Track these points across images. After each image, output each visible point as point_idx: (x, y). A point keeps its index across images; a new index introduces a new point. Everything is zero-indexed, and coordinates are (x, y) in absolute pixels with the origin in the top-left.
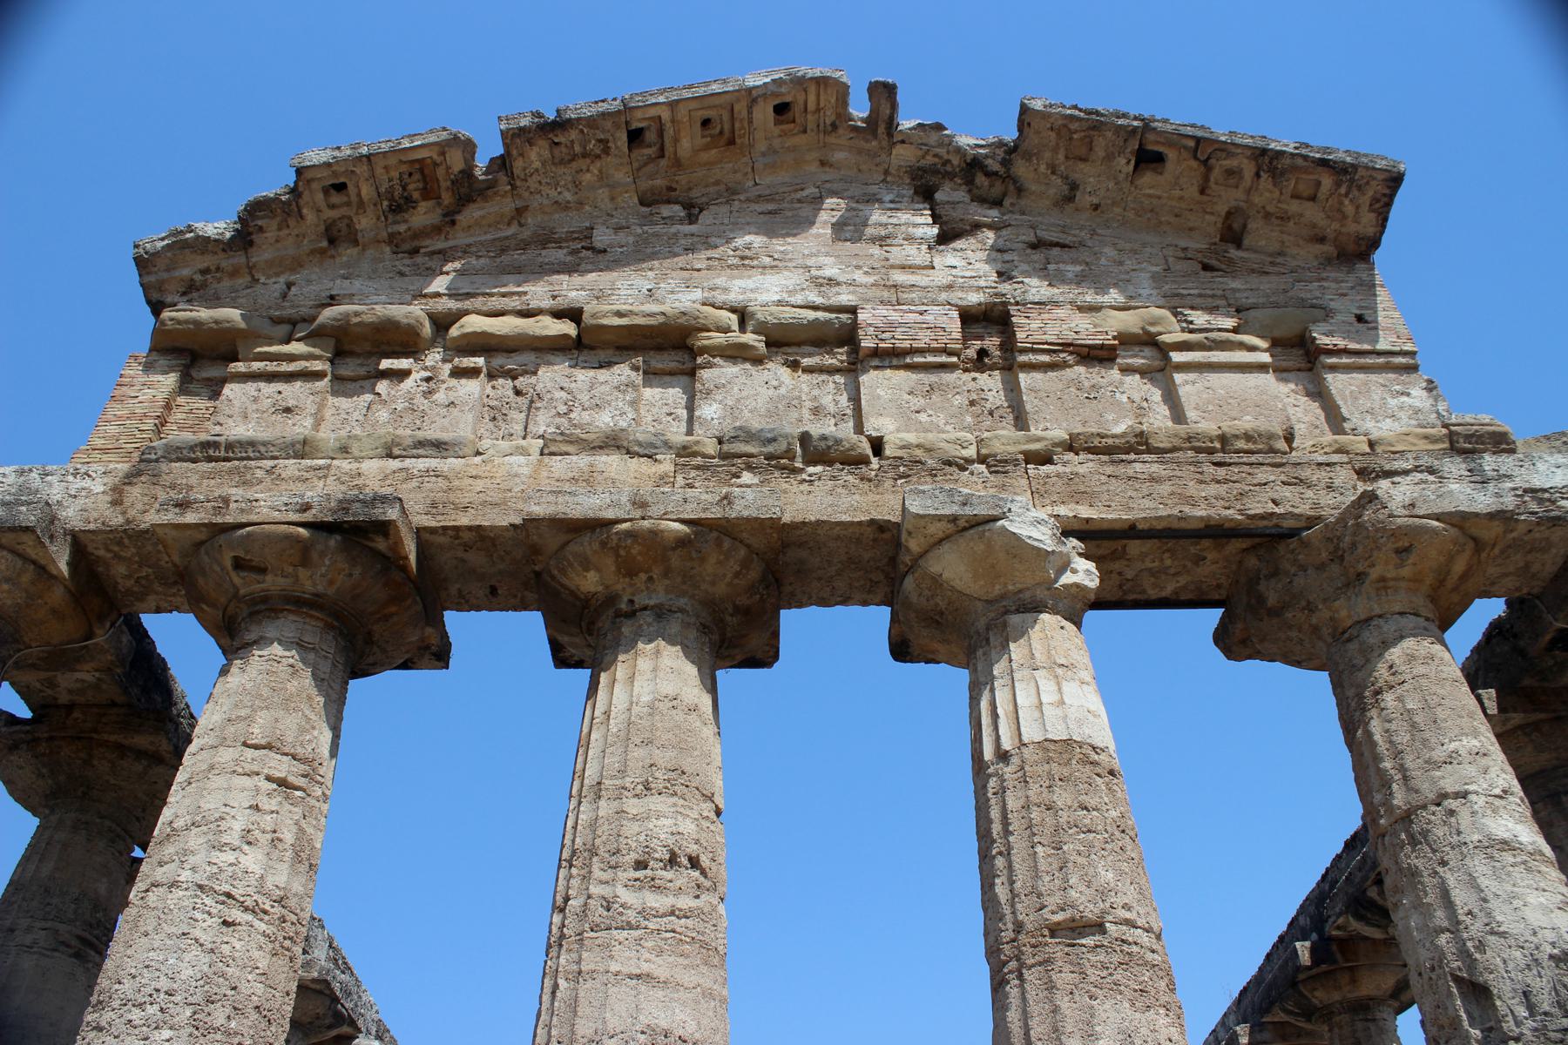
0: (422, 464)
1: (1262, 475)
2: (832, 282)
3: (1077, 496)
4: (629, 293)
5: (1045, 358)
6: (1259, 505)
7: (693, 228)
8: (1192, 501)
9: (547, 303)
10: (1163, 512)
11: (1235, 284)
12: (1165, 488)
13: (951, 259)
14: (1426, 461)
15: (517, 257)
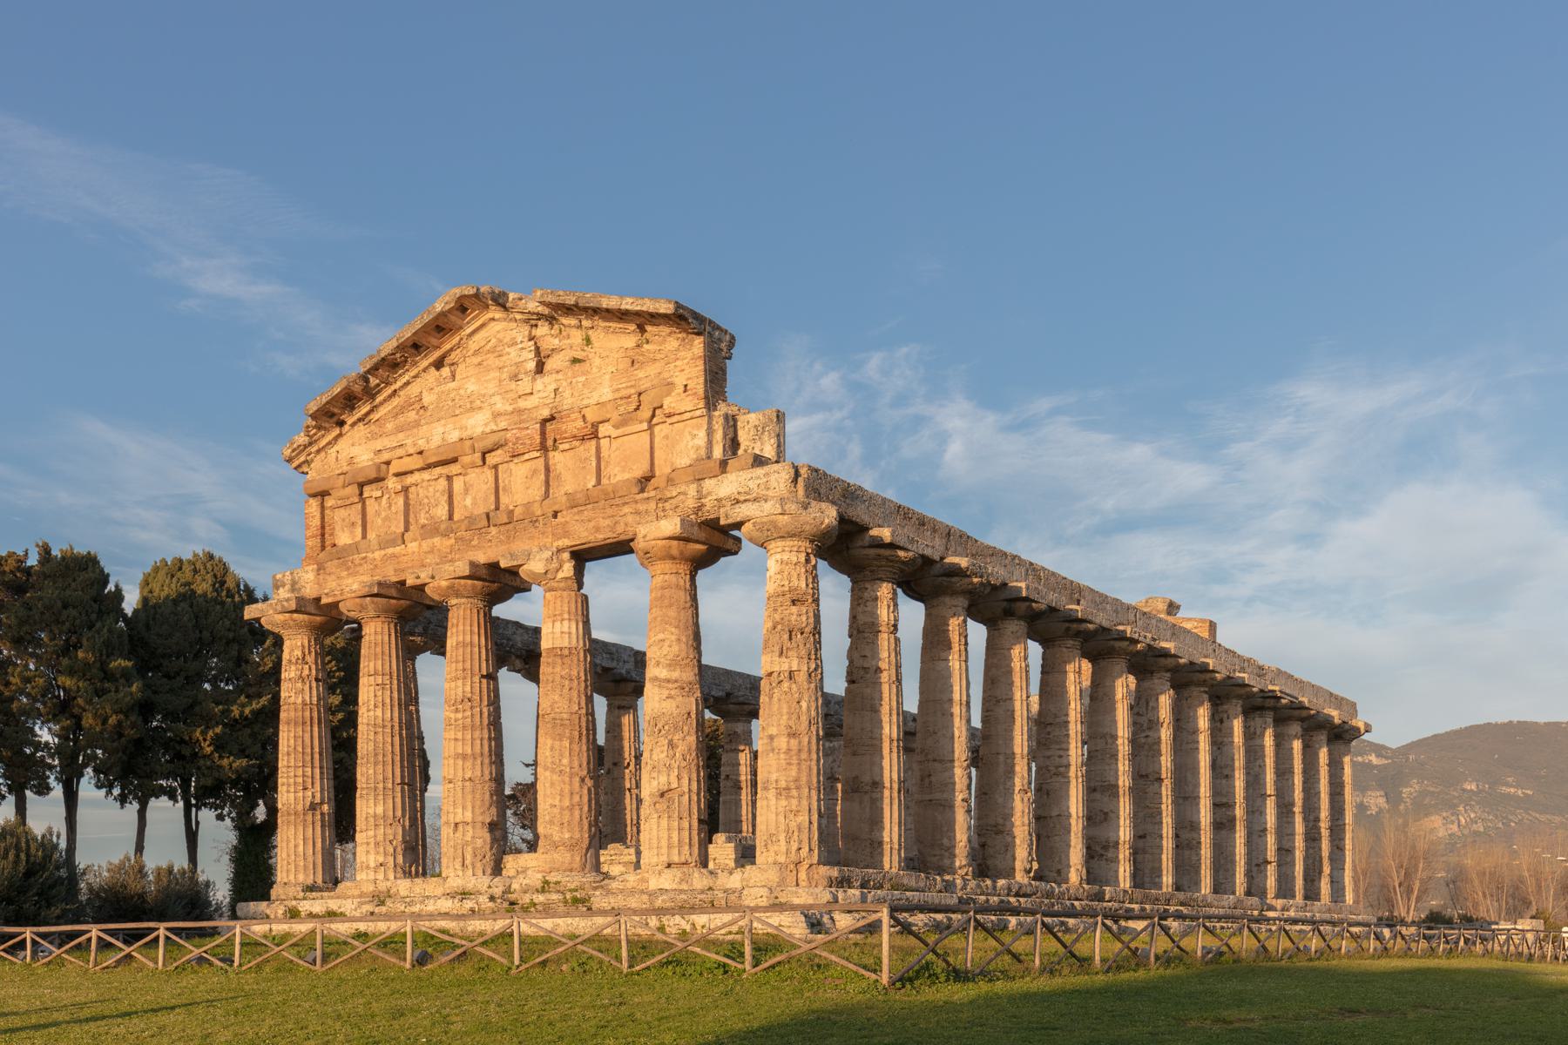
0: (390, 551)
1: (626, 509)
2: (499, 414)
3: (566, 534)
4: (438, 435)
5: (566, 446)
6: (620, 529)
7: (452, 385)
8: (597, 529)
9: (411, 451)
10: (592, 538)
11: (641, 374)
12: (592, 524)
13: (540, 382)
14: (683, 488)
15: (401, 419)
